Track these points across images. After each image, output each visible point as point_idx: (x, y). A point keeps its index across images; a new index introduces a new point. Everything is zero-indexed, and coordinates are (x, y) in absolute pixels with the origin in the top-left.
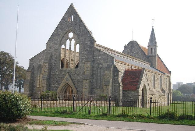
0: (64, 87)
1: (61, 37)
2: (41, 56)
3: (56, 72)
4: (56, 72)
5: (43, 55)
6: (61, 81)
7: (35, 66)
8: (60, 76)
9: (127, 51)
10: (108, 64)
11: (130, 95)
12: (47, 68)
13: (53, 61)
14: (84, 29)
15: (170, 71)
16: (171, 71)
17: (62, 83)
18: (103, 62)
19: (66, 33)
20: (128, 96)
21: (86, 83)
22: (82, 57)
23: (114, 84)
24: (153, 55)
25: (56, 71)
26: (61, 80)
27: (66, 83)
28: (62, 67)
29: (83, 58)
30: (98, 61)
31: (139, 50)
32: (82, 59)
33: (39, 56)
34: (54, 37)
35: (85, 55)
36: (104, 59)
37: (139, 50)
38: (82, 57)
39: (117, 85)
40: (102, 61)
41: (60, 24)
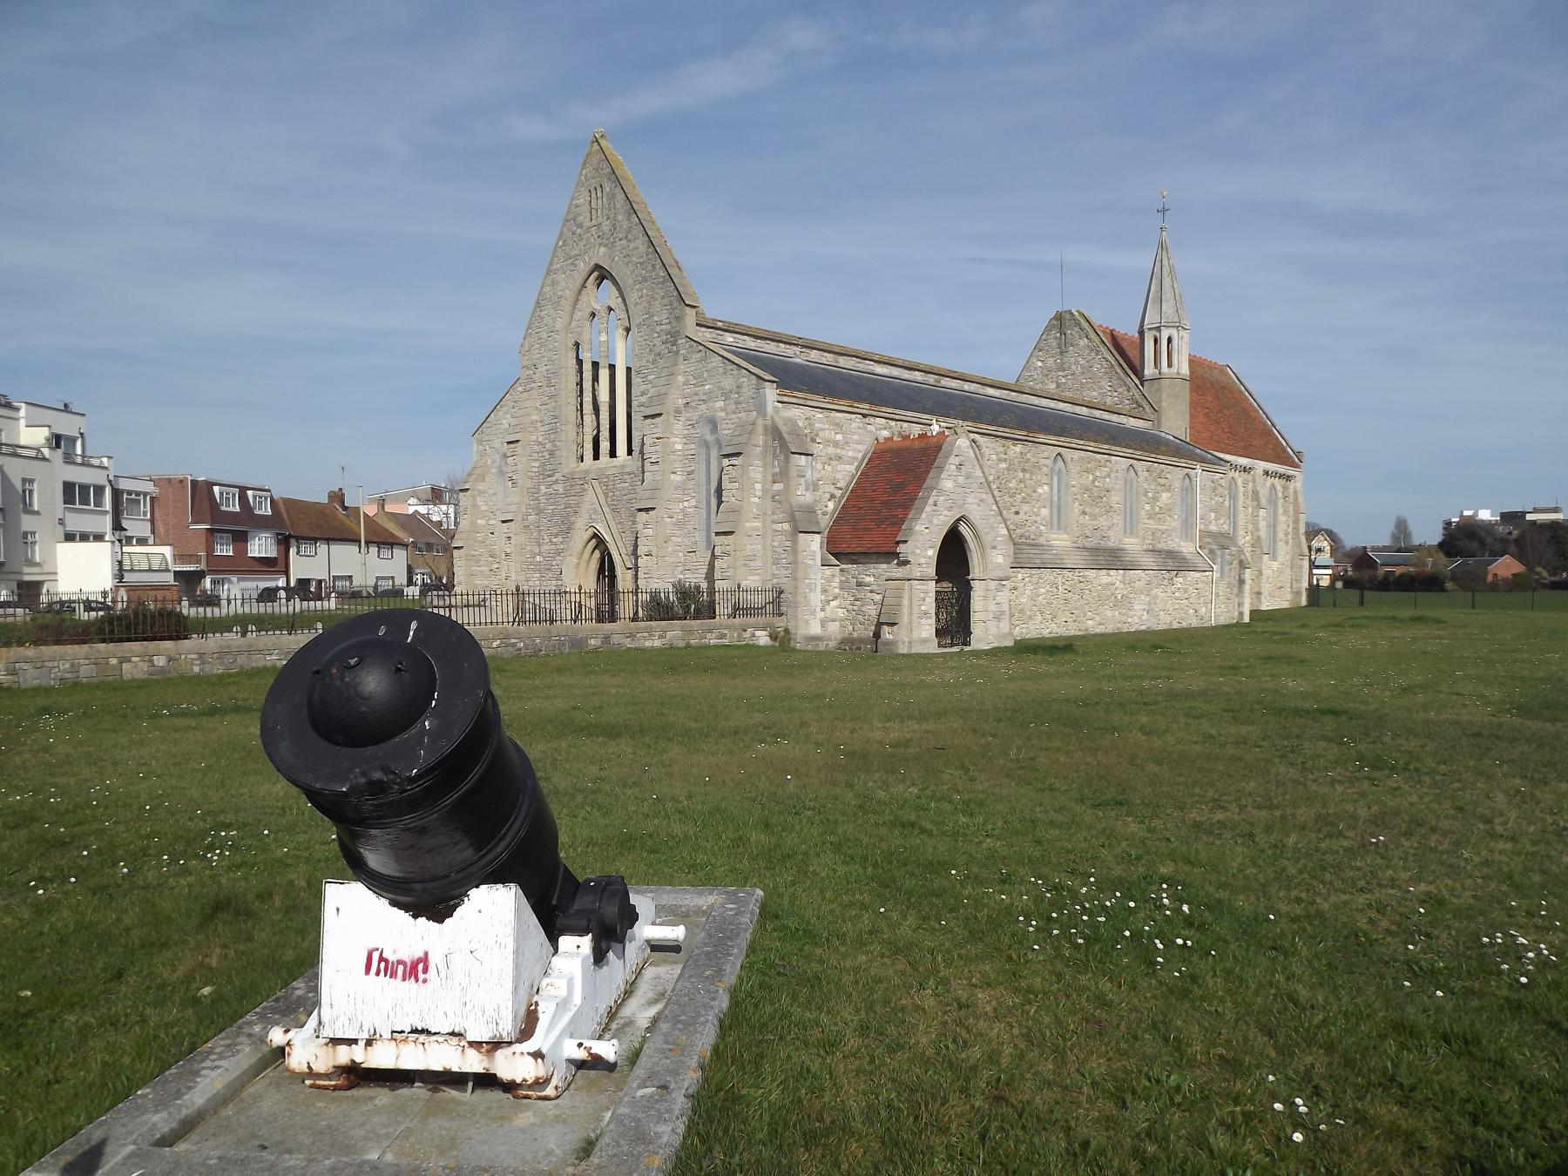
1: (567, 305)
11: (868, 579)
14: (643, 249)
15: (1296, 450)
16: (1298, 454)
18: (723, 410)
19: (584, 286)
20: (859, 584)
33: (501, 413)
34: (543, 314)
36: (726, 396)
39: (786, 526)
41: (561, 243)
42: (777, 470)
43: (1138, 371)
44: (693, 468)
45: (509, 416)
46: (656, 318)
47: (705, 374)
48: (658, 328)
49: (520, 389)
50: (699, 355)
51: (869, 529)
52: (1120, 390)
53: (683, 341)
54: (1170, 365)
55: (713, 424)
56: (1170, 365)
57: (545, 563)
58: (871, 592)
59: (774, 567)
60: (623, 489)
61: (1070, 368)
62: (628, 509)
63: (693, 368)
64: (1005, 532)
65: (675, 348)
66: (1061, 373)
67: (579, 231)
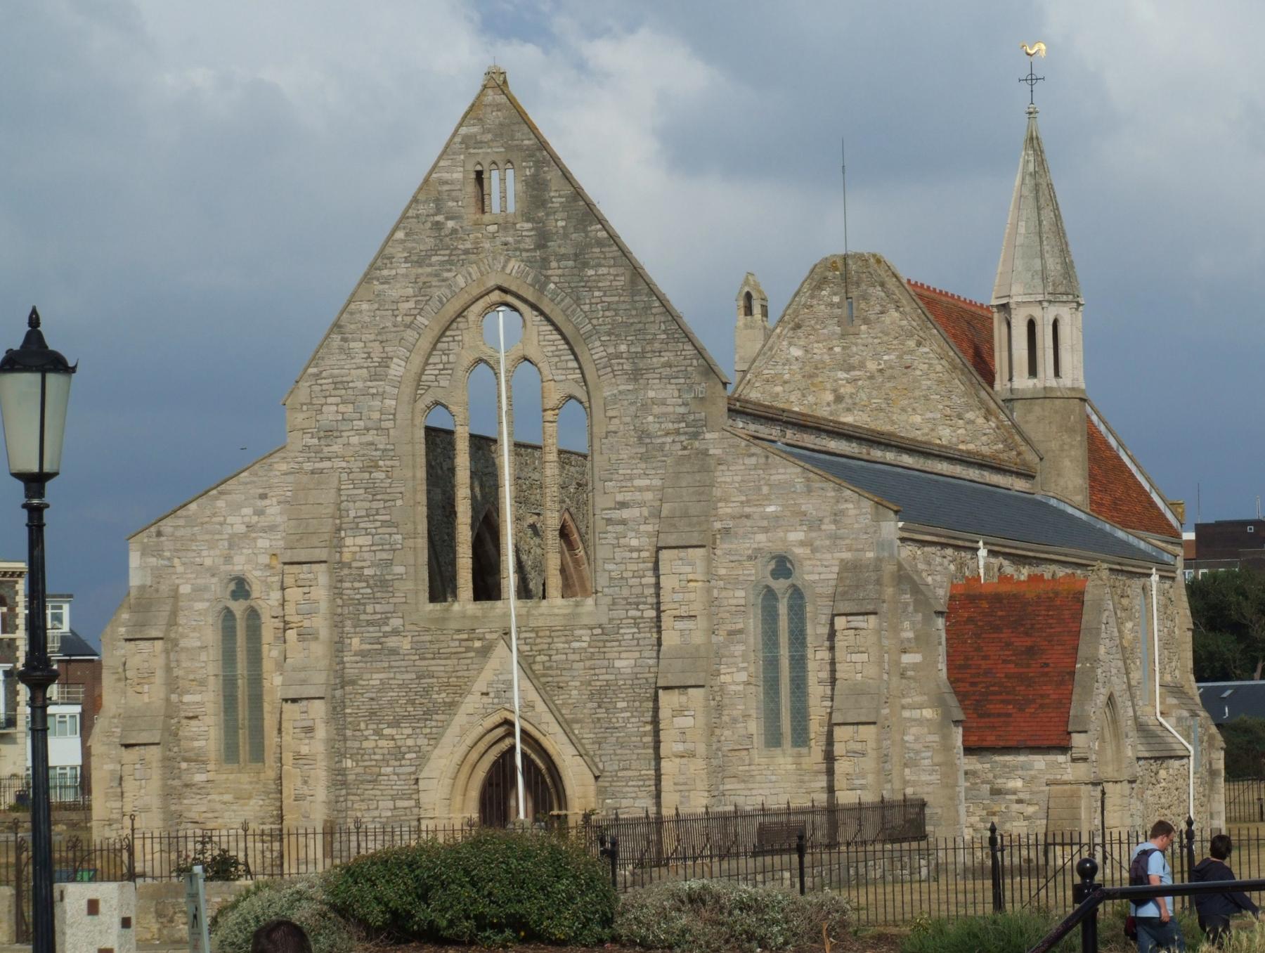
0: (474, 756)
1: (425, 344)
2: (240, 506)
3: (396, 632)
4: (396, 632)
5: (263, 497)
6: (451, 706)
7: (185, 589)
8: (437, 666)
9: (796, 352)
10: (842, 560)
11: (1011, 784)
12: (324, 606)
13: (361, 540)
17: (460, 719)
18: (802, 544)
20: (996, 792)
21: (679, 712)
22: (623, 505)
23: (903, 707)
24: (1052, 382)
25: (396, 622)
26: (441, 697)
27: (496, 718)
28: (441, 587)
29: (625, 514)
30: (761, 537)
31: (911, 344)
32: (623, 522)
33: (221, 504)
35: (640, 489)
36: (814, 525)
37: (911, 344)
38: (623, 505)
40: (796, 536)
41: (400, 235)
42: (911, 635)
43: (988, 375)
44: (740, 626)
45: (247, 511)
46: (651, 394)
47: (765, 490)
48: (656, 410)
49: (284, 467)
50: (753, 460)
51: (1009, 715)
52: (970, 415)
53: (715, 435)
54: (1057, 373)
55: (783, 566)
56: (1057, 373)
57: (360, 770)
58: (1020, 801)
59: (907, 771)
60: (574, 651)
61: (862, 365)
62: (589, 684)
63: (738, 478)
64: (1131, 713)
65: (697, 444)
66: (841, 375)
67: (450, 224)
